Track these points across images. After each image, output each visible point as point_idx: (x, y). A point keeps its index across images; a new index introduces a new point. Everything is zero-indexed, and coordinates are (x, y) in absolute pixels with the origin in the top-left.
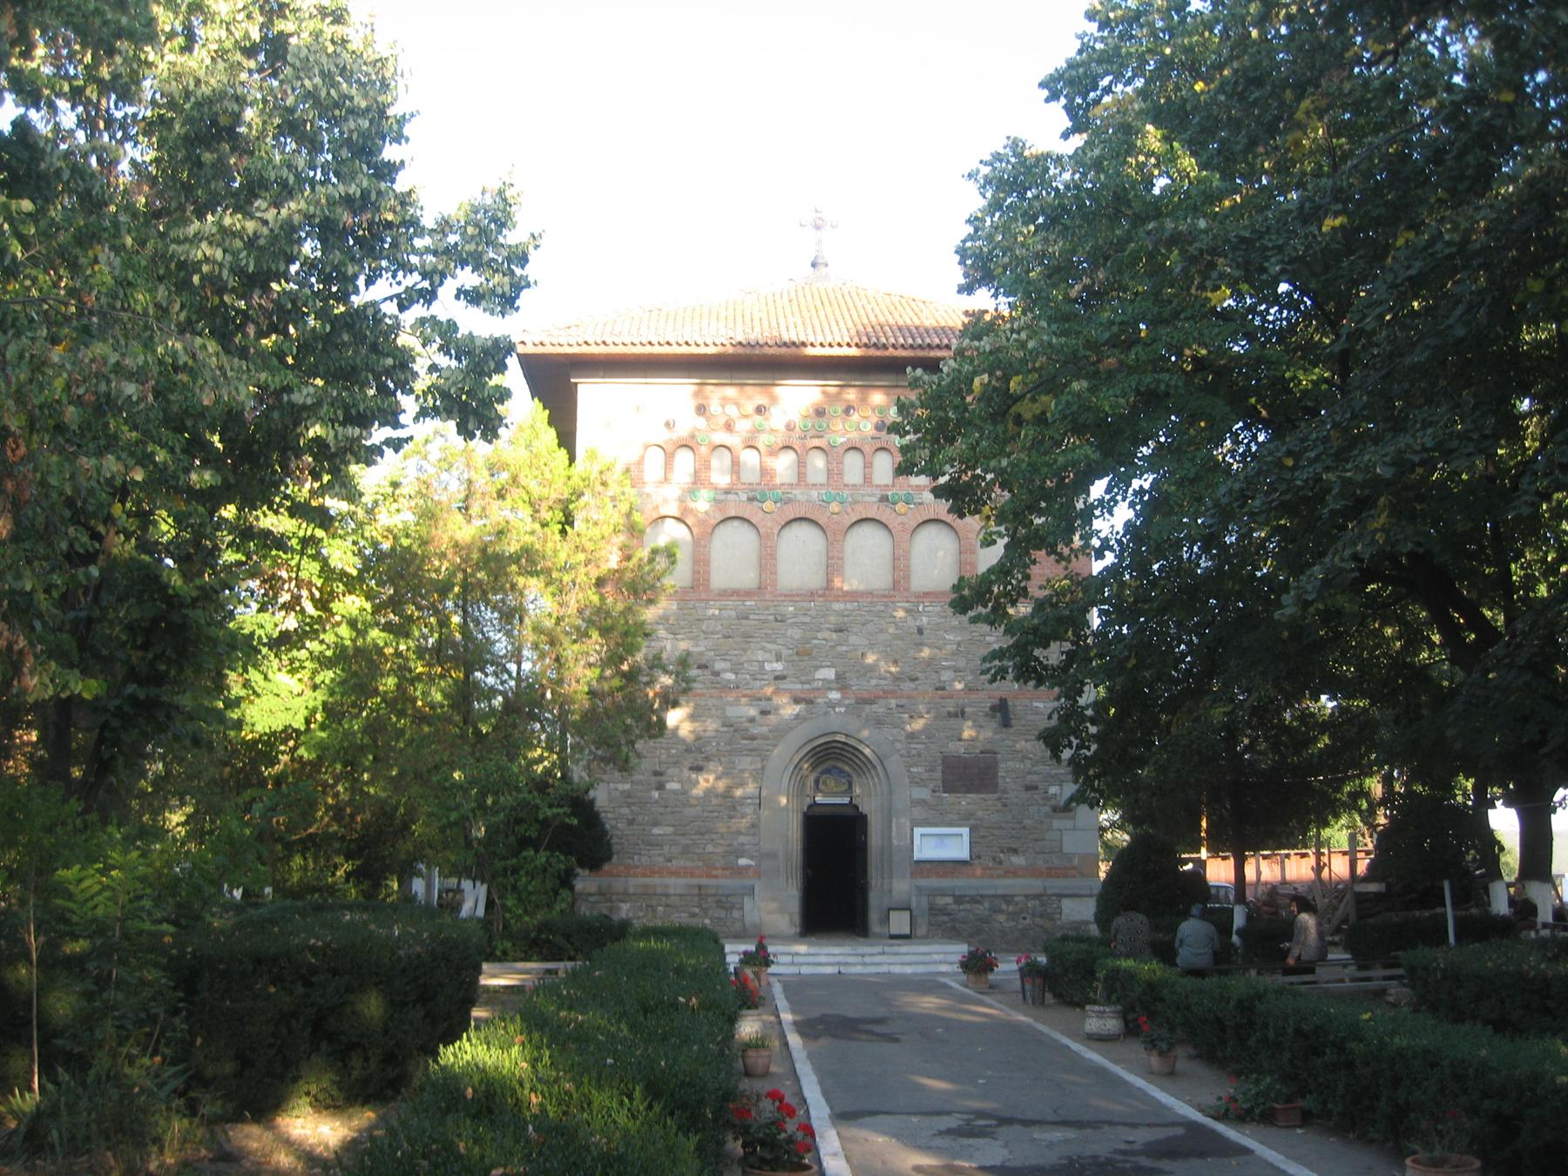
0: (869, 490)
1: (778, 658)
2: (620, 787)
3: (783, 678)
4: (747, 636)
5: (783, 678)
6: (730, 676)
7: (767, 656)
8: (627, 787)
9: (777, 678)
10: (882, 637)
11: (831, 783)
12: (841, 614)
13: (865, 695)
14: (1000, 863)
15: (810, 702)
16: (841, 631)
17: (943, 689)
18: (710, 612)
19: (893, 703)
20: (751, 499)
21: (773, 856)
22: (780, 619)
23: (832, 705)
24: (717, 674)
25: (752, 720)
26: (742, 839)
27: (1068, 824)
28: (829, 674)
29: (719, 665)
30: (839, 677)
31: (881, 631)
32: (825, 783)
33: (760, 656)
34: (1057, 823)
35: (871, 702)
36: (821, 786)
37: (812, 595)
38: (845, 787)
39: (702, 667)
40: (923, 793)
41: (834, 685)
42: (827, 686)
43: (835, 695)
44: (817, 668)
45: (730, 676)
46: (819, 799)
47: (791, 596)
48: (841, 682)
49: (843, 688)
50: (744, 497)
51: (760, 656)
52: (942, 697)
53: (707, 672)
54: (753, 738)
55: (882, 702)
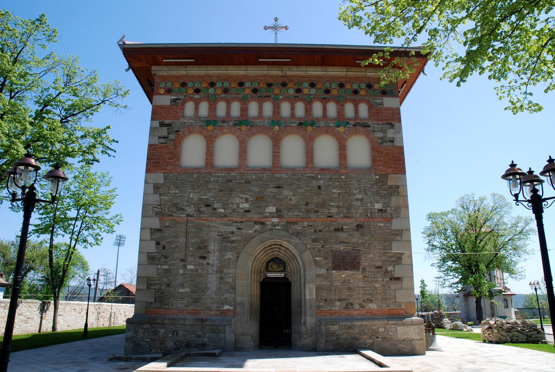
0: (293, 120)
1: (247, 201)
2: (164, 267)
3: (249, 211)
4: (231, 190)
5: (249, 211)
6: (223, 211)
7: (241, 200)
8: (167, 267)
9: (246, 211)
10: (300, 191)
11: (275, 266)
12: (279, 179)
13: (291, 220)
14: (364, 307)
15: (263, 223)
16: (279, 187)
17: (331, 217)
18: (212, 179)
19: (306, 224)
20: (235, 125)
21: (242, 304)
22: (248, 182)
23: (274, 225)
24: (215, 209)
25: (233, 233)
26: (226, 295)
27: (399, 286)
28: (272, 209)
29: (215, 206)
30: (278, 211)
31: (299, 188)
32: (271, 266)
33: (237, 200)
34: (393, 286)
35: (295, 223)
36: (269, 268)
37: (264, 169)
38: (281, 269)
39: (208, 206)
40: (323, 271)
41: (276, 215)
42: (272, 215)
43: (276, 220)
44: (267, 206)
45: (223, 211)
46: (270, 275)
47: (254, 170)
48: (279, 214)
49: (279, 217)
50: (231, 124)
51: (237, 200)
52: (331, 221)
53: (210, 209)
54: (233, 242)
55: (301, 223)
